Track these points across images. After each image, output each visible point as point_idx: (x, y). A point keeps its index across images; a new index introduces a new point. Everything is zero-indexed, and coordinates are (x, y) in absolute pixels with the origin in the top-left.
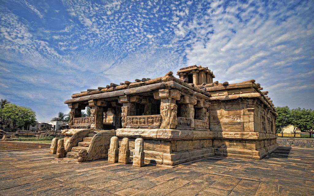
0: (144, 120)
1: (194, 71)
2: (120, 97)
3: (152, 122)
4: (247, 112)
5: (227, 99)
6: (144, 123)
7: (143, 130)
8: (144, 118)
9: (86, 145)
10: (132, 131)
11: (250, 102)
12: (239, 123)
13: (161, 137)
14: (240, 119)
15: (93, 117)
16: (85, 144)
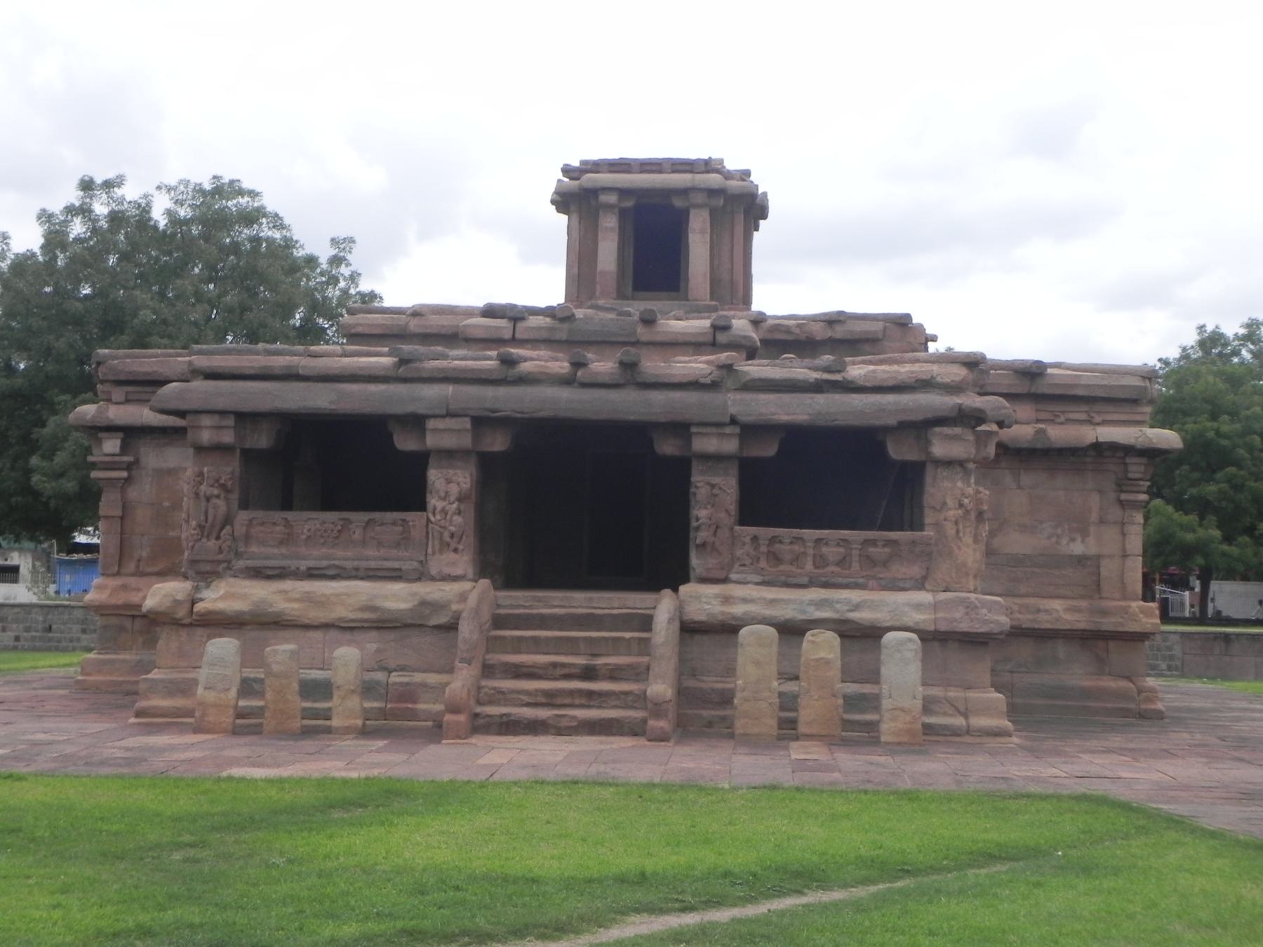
0: (842, 550)
1: (699, 198)
2: (694, 430)
3: (885, 564)
4: (1115, 513)
5: (1039, 446)
6: (842, 563)
7: (854, 596)
8: (844, 542)
9: (559, 672)
10: (788, 601)
11: (1137, 468)
12: (1081, 560)
13: (962, 625)
14: (1083, 541)
15: (458, 519)
16: (555, 665)
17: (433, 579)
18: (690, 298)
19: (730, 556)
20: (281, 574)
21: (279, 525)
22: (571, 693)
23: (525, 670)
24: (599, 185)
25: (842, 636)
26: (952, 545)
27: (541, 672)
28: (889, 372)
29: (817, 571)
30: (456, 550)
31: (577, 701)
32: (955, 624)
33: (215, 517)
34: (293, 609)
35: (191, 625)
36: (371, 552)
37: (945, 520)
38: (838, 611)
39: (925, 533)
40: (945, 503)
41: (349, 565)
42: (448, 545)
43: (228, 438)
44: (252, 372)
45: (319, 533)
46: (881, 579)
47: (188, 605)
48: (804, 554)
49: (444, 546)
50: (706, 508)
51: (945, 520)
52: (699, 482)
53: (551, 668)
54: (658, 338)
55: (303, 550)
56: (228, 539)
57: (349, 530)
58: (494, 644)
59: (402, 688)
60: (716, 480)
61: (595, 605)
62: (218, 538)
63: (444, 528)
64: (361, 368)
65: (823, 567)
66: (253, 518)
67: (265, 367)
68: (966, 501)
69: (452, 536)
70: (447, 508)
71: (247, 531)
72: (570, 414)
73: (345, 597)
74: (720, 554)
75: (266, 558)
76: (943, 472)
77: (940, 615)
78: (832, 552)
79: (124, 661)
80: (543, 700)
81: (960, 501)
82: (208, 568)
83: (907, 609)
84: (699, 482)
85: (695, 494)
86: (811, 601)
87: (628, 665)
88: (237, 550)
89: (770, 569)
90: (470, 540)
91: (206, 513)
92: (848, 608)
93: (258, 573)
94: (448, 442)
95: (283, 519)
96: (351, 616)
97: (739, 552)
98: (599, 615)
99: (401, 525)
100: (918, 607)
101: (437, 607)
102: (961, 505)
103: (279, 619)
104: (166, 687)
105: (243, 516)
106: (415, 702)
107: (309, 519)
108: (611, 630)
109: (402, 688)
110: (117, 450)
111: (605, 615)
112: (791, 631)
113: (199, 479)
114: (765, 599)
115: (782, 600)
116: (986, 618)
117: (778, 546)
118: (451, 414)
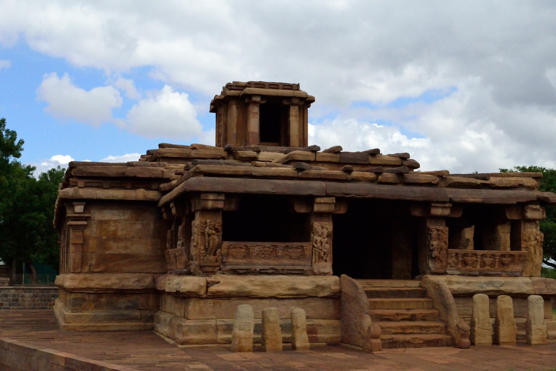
0: (492, 259)
1: (296, 101)
3: (507, 265)
6: (492, 265)
7: (501, 280)
9: (400, 317)
15: (327, 246)
16: (398, 314)
17: (315, 274)
18: (291, 145)
19: (446, 262)
20: (247, 272)
21: (242, 248)
22: (413, 327)
23: (386, 317)
24: (253, 93)
25: (512, 297)
26: (533, 256)
27: (392, 318)
28: (507, 181)
29: (481, 269)
30: (326, 261)
31: (416, 331)
32: (542, 291)
33: (213, 244)
34: (257, 290)
35: (207, 298)
36: (285, 261)
37: (530, 245)
38: (496, 287)
39: (522, 251)
40: (530, 238)
41: (279, 268)
42: (322, 258)
43: (220, 205)
44: (229, 173)
45: (261, 252)
46: (507, 272)
47: (205, 288)
48: (477, 261)
49: (320, 258)
50: (436, 241)
51: (530, 245)
52: (433, 228)
53: (396, 316)
54: (378, 163)
55: (255, 261)
56: (220, 255)
57: (276, 250)
58: (374, 305)
59: (310, 327)
60: (441, 228)
61: (393, 286)
63: (321, 250)
64: (282, 173)
65: (483, 267)
67: (236, 171)
68: (538, 237)
70: (322, 241)
72: (381, 197)
73: (280, 283)
74: (441, 261)
75: (237, 265)
76: (528, 225)
77: (535, 287)
78: (488, 260)
79: (87, 316)
80: (400, 331)
81: (535, 237)
82: (210, 269)
83: (523, 285)
84: (433, 228)
85: (431, 234)
86: (484, 282)
87: (430, 314)
88: (222, 261)
89: (463, 268)
90: (329, 257)
92: (499, 285)
93: (235, 272)
94: (324, 208)
95: (245, 245)
96: (284, 292)
97: (450, 261)
98: (403, 291)
100: (527, 284)
101: (323, 287)
102: (536, 239)
103: (249, 295)
104: (196, 329)
105: (226, 244)
106: (316, 334)
107: (257, 245)
108: (408, 297)
109: (310, 327)
110: (82, 211)
111: (405, 290)
112: (493, 296)
113: (205, 225)
114: (465, 282)
115: (473, 282)
116: (554, 288)
117: (466, 257)
118: (327, 196)
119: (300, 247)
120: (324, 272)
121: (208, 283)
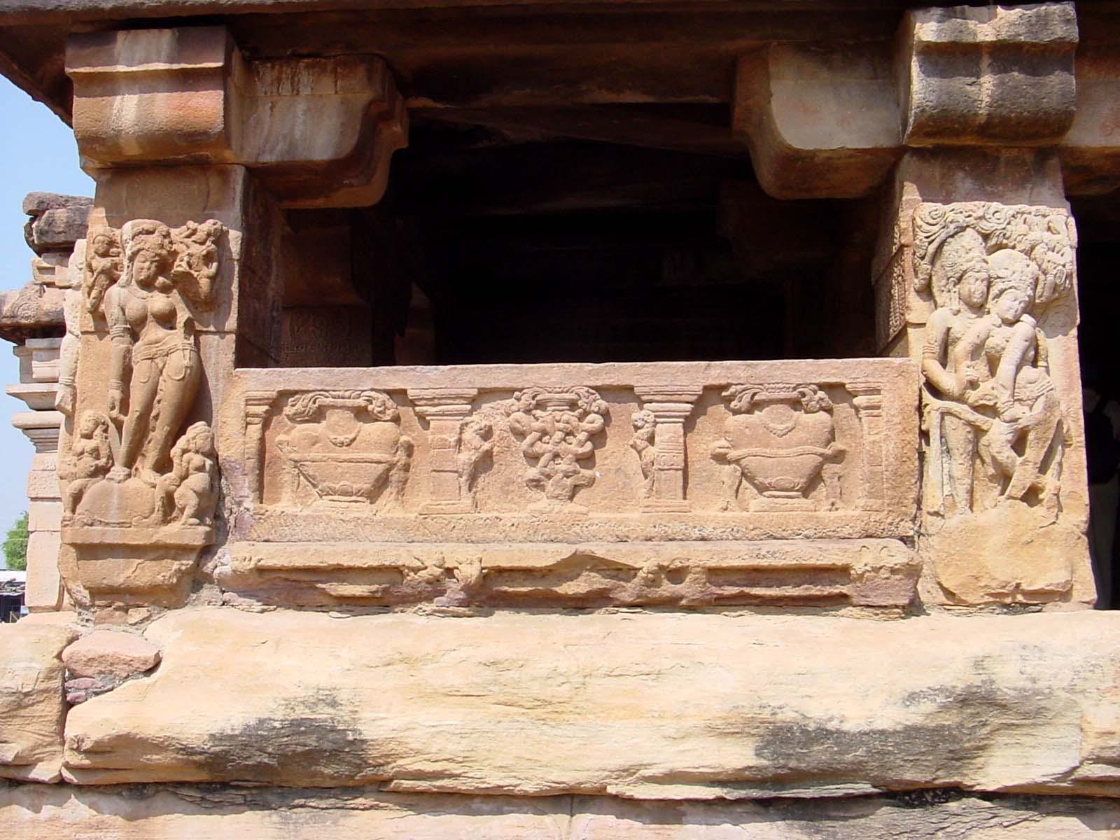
47: (51, 708)
56: (200, 469)
62: (163, 465)
63: (991, 411)
66: (285, 395)
69: (1019, 444)
71: (262, 440)
91: (126, 374)
99: (829, 411)
113: (106, 262)
119: (821, 394)
120: (1024, 587)
121: (66, 672)
